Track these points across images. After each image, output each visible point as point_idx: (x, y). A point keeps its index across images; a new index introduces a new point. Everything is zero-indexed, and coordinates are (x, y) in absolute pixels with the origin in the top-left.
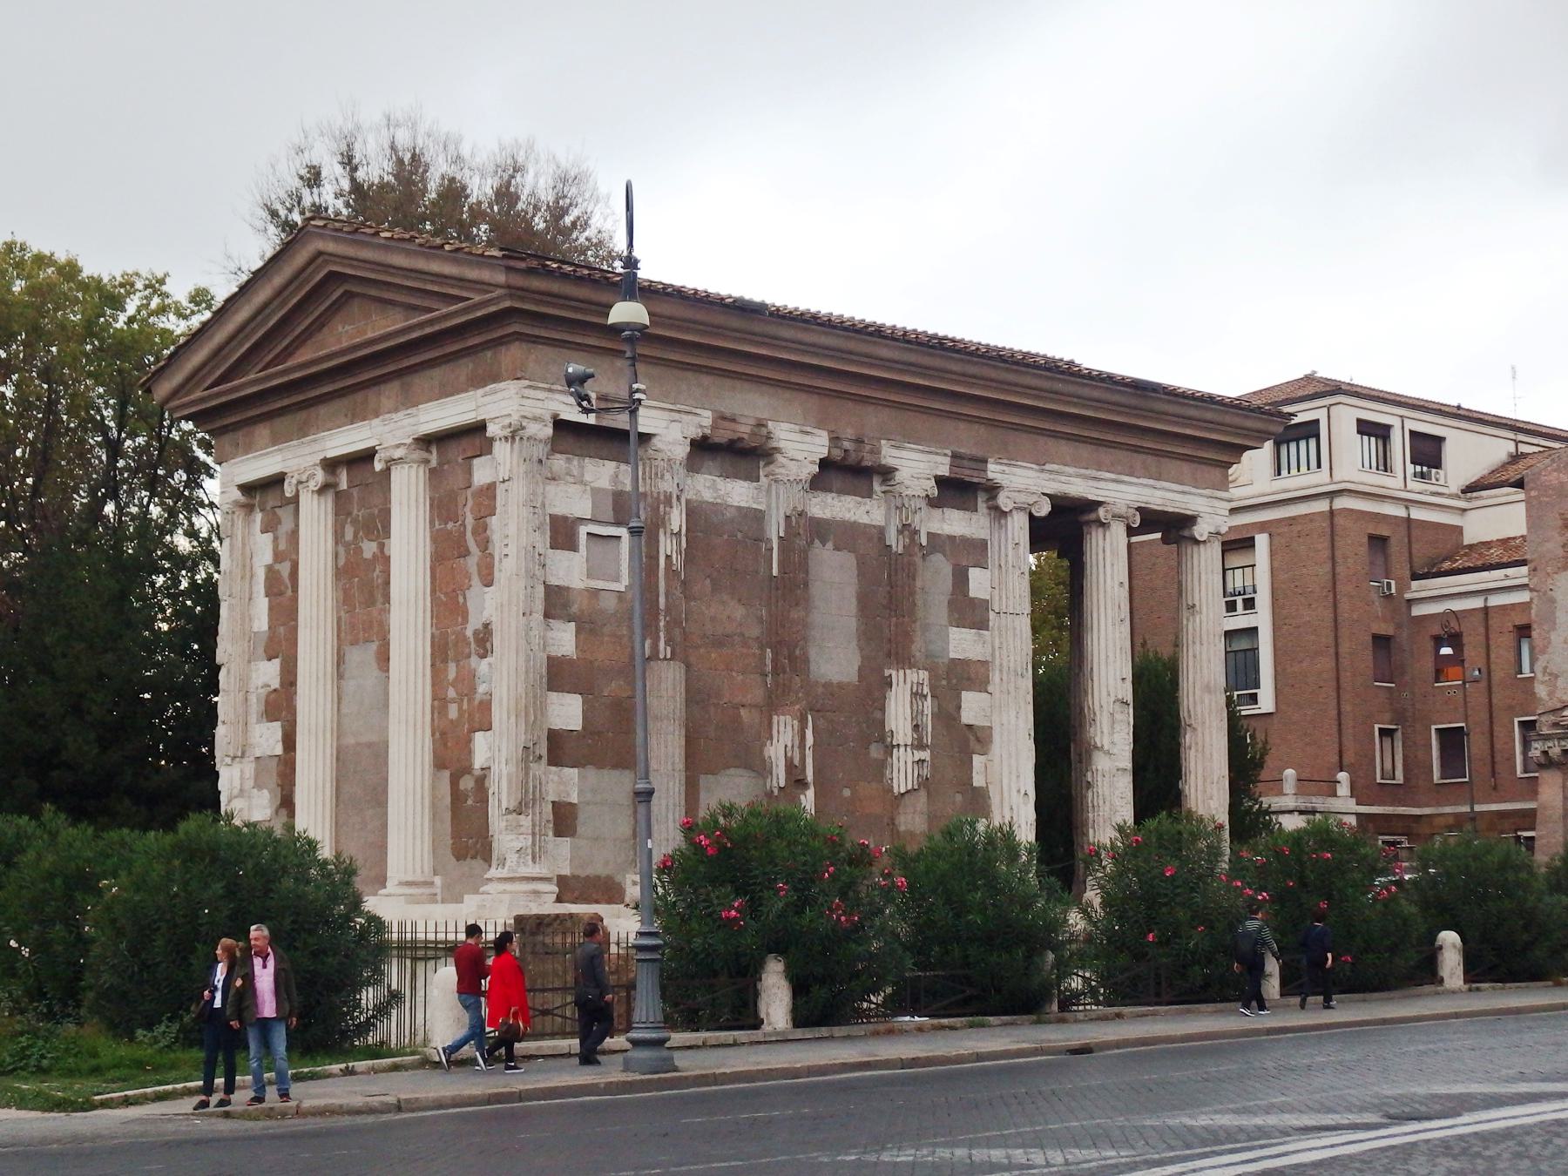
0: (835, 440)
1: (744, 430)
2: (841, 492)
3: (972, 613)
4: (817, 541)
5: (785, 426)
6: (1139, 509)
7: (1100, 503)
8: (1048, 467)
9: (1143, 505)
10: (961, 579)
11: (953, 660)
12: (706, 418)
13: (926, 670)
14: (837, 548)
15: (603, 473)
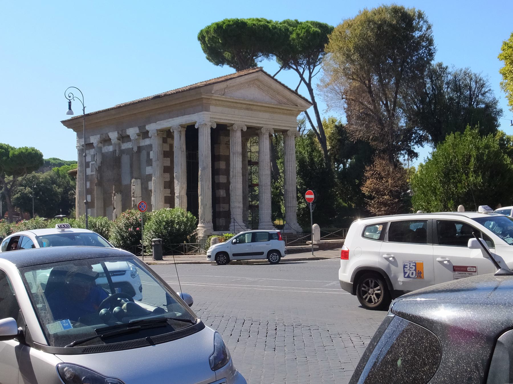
0: (118, 133)
1: (104, 136)
2: (127, 142)
3: (149, 162)
4: (123, 155)
5: (110, 133)
6: (180, 125)
7: (171, 127)
8: (158, 122)
9: (181, 124)
10: (148, 154)
11: (147, 175)
12: (99, 136)
13: (140, 179)
14: (126, 155)
15: (92, 152)
